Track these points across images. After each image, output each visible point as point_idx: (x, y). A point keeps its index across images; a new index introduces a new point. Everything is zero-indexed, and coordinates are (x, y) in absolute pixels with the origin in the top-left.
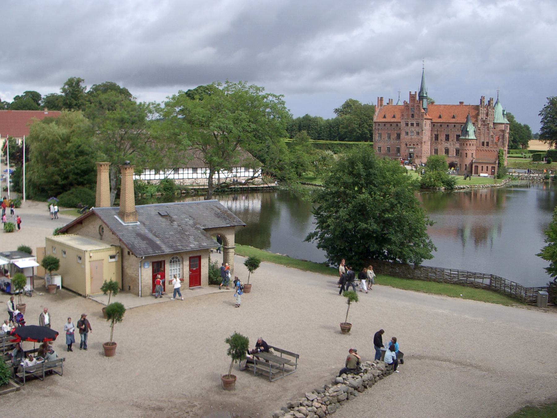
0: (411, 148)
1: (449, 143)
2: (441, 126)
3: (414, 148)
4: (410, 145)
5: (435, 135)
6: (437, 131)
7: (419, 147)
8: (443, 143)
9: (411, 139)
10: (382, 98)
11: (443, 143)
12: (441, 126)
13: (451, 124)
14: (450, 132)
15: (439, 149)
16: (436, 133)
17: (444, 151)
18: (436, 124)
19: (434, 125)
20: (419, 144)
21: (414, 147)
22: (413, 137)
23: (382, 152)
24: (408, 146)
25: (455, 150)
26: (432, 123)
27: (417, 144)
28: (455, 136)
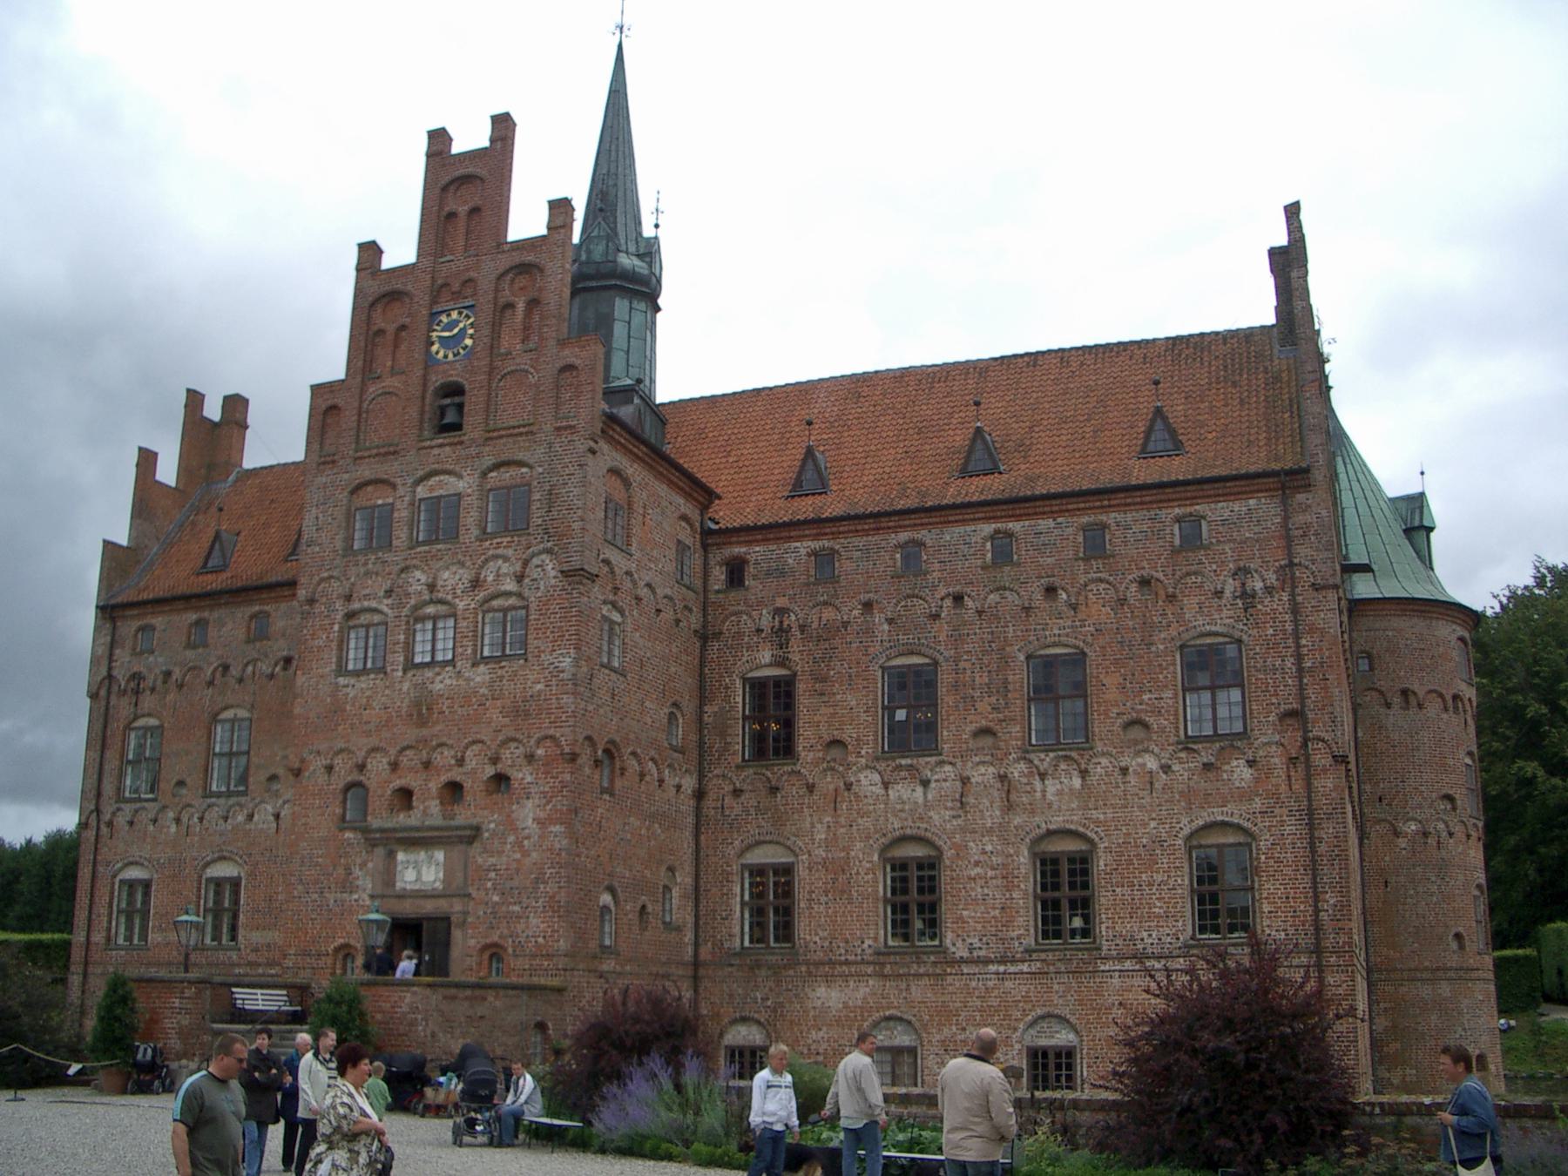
0: (417, 841)
1: (945, 777)
2: (825, 559)
3: (473, 835)
4: (405, 796)
5: (758, 688)
6: (781, 635)
7: (528, 814)
8: (868, 782)
9: (423, 710)
10: (236, 405)
11: (868, 782)
12: (825, 559)
13: (952, 534)
14: (942, 630)
15: (801, 872)
16: (763, 662)
17: (881, 885)
18: (756, 552)
19: (736, 573)
20: (523, 776)
21: (464, 816)
22: (442, 683)
23: (153, 937)
24: (375, 822)
25: (1024, 859)
26: (710, 537)
27: (501, 780)
28: (1020, 677)
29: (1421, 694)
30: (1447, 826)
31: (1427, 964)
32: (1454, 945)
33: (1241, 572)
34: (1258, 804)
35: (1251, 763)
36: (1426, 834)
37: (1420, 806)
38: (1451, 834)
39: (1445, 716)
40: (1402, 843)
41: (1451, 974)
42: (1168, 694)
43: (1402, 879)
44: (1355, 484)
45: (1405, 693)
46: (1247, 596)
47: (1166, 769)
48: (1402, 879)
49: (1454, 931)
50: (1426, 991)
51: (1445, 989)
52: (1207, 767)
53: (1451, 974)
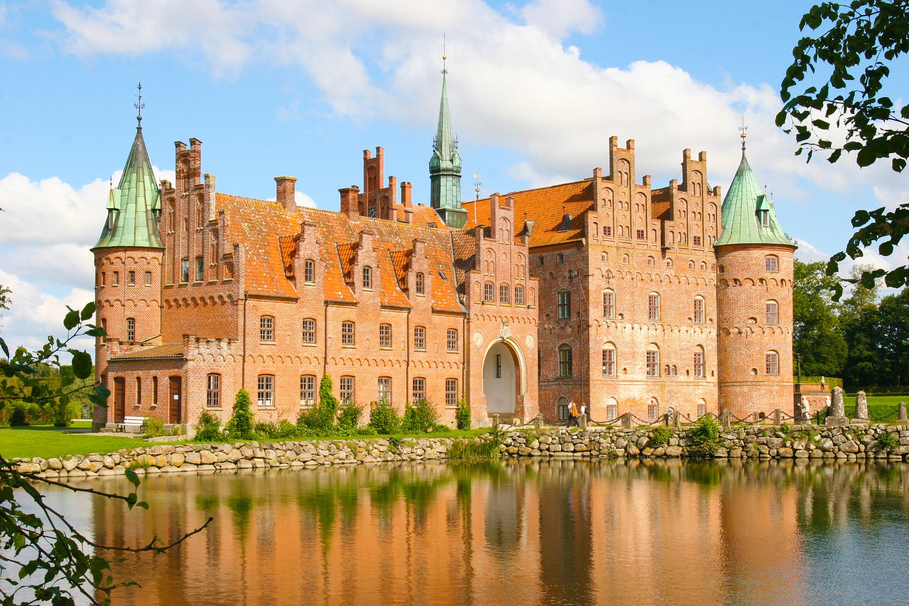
29: (741, 281)
30: (751, 330)
31: (739, 380)
32: (753, 373)
33: (570, 271)
34: (572, 338)
35: (570, 327)
36: (740, 333)
37: (739, 322)
38: (752, 332)
39: (753, 287)
40: (732, 336)
41: (750, 384)
42: (554, 307)
43: (731, 349)
44: (740, 193)
45: (736, 280)
46: (571, 278)
47: (554, 328)
48: (731, 349)
49: (752, 368)
50: (738, 389)
51: (745, 389)
52: (562, 328)
53: (750, 384)
